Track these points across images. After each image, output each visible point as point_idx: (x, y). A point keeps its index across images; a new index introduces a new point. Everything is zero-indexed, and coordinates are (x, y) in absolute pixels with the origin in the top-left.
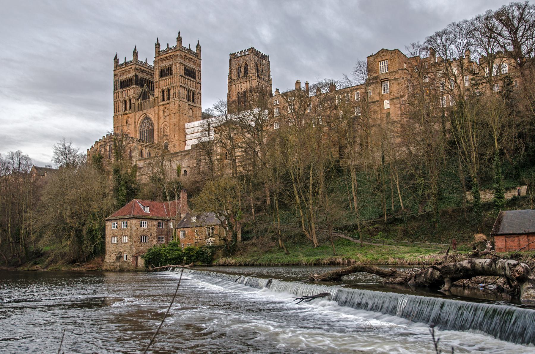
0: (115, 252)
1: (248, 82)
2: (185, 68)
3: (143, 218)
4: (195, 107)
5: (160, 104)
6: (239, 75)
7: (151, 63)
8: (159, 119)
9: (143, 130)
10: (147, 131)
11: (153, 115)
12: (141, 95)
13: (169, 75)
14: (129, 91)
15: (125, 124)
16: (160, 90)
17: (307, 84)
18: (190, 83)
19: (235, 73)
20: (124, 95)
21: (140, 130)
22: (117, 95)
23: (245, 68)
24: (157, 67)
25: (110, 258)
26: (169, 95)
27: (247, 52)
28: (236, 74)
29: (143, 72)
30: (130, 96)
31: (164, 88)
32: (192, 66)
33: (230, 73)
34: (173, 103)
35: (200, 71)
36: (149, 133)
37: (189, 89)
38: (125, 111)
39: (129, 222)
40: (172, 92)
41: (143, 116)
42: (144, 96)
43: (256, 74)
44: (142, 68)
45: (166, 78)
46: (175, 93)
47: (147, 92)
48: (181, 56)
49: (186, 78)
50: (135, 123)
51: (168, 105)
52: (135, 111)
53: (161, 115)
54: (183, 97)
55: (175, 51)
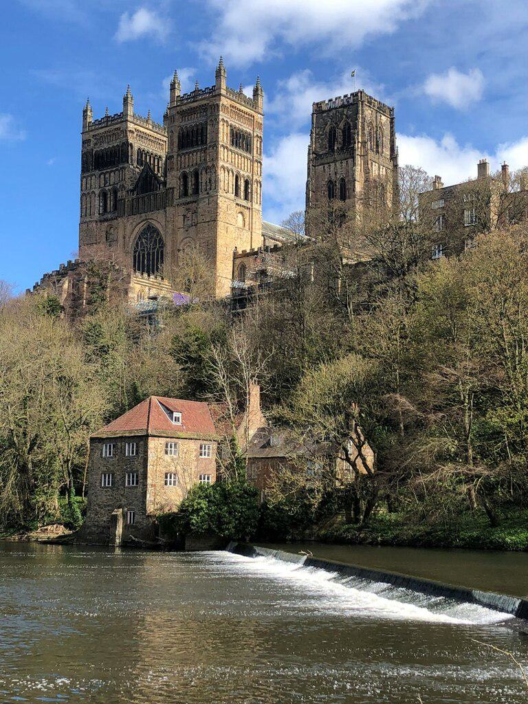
2: (232, 130)
10: (149, 254)
11: (163, 223)
12: (137, 183)
13: (197, 145)
14: (112, 174)
21: (135, 252)
23: (344, 132)
26: (197, 184)
30: (114, 184)
36: (153, 259)
37: (238, 172)
38: (103, 215)
40: (204, 178)
41: (141, 225)
44: (141, 129)
46: (210, 180)
47: (151, 177)
50: (124, 238)
54: (226, 188)
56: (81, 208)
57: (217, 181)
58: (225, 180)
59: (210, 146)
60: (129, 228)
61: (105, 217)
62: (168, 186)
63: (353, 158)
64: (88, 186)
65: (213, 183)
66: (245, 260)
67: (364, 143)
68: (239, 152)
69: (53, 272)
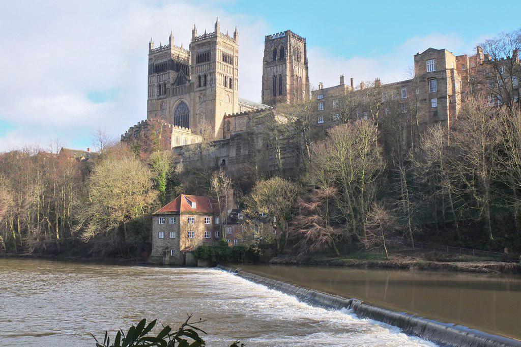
2: (223, 54)
6: (274, 58)
8: (194, 105)
9: (178, 115)
10: (182, 116)
11: (189, 100)
14: (164, 76)
15: (159, 109)
17: (352, 80)
23: (281, 51)
27: (283, 34)
28: (272, 56)
32: (230, 53)
33: (265, 56)
40: (209, 78)
42: (180, 81)
47: (183, 78)
54: (220, 83)
57: (215, 79)
58: (219, 79)
59: (212, 62)
60: (172, 103)
61: (160, 97)
63: (286, 64)
65: (214, 81)
66: (230, 119)
67: (291, 56)
69: (135, 126)
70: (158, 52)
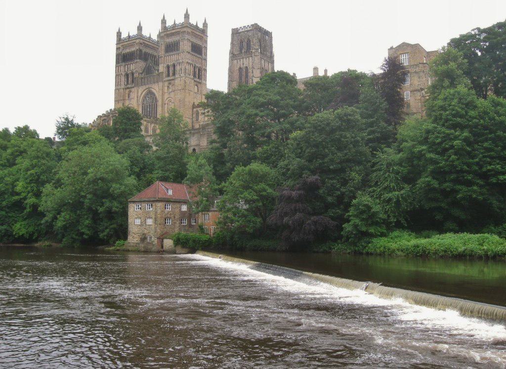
0: (139, 233)
1: (251, 58)
2: (192, 45)
3: (167, 201)
4: (200, 83)
5: (164, 79)
6: (241, 49)
7: (155, 37)
8: (163, 95)
10: (150, 105)
13: (175, 50)
14: (131, 65)
15: (127, 98)
16: (165, 65)
17: (326, 71)
18: (197, 59)
19: (237, 48)
20: (126, 68)
22: (120, 68)
23: (247, 44)
24: (163, 43)
25: (133, 239)
29: (147, 46)
31: (170, 64)
32: (199, 43)
34: (179, 79)
35: (206, 48)
38: (127, 85)
39: (154, 204)
40: (178, 68)
42: (148, 71)
43: (259, 50)
45: (172, 54)
46: (181, 69)
48: (188, 33)
49: (192, 54)
50: (138, 97)
51: (173, 81)
52: (137, 85)
53: (166, 90)
55: (182, 28)
56: (116, 82)
62: (160, 71)
64: (119, 71)
66: (198, 109)
68: (194, 54)
70: (126, 41)
